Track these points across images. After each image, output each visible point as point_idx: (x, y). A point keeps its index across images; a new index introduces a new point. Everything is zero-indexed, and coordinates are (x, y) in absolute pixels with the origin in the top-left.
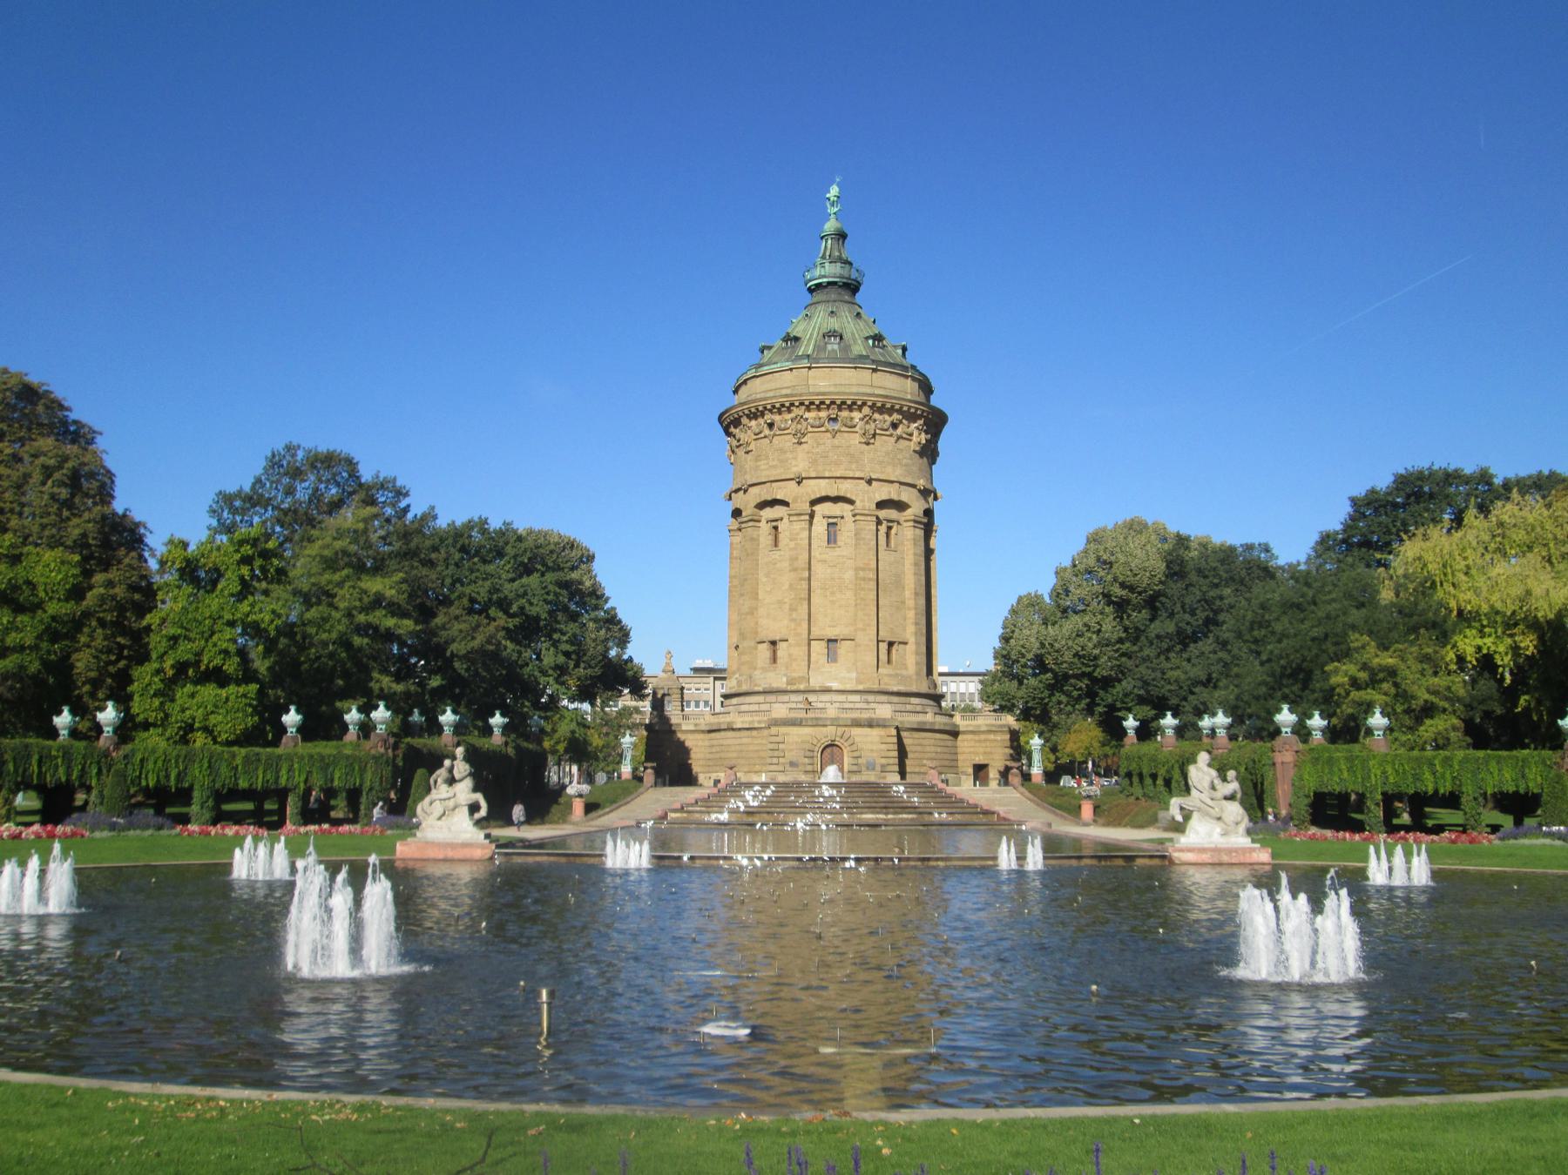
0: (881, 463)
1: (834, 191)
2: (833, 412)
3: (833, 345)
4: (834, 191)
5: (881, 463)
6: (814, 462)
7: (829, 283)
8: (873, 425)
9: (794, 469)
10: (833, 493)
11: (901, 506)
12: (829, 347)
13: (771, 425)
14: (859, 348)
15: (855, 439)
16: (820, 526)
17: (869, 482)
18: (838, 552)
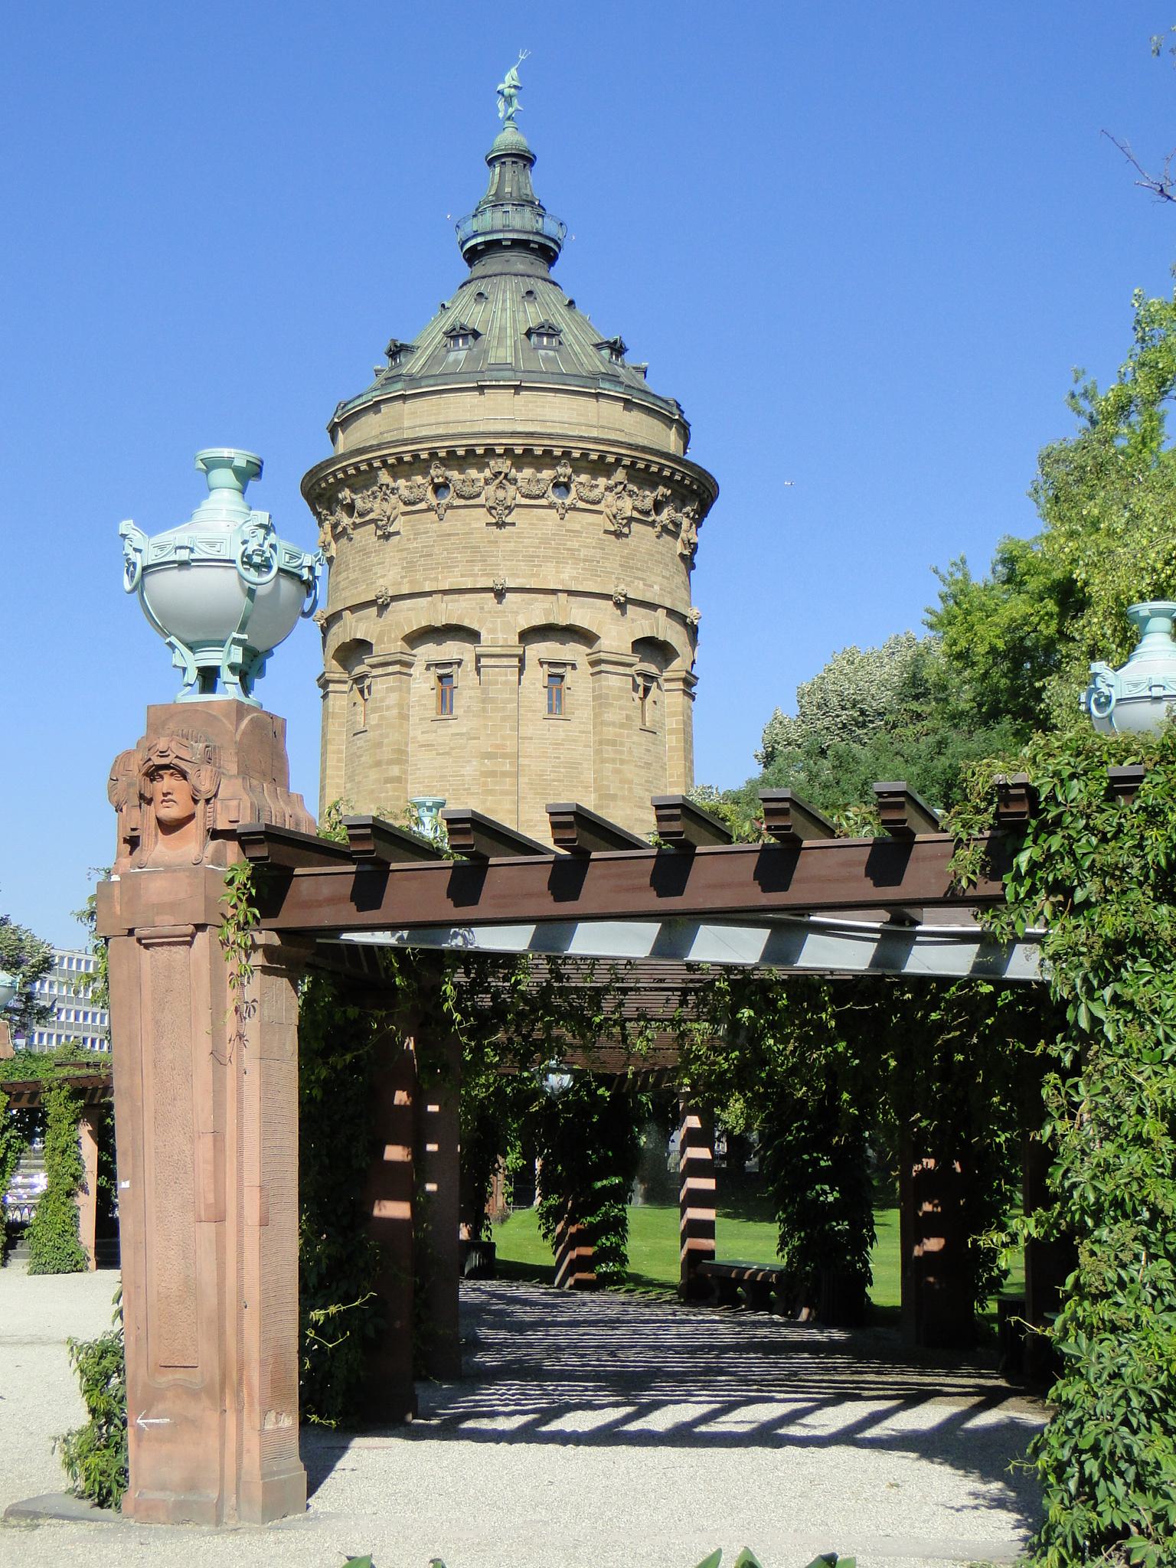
0: (530, 558)
1: (511, 77)
2: (437, 472)
3: (460, 354)
4: (511, 77)
5: (530, 558)
6: (410, 567)
7: (485, 243)
8: (511, 489)
9: (381, 581)
10: (440, 621)
11: (585, 637)
12: (452, 356)
13: (350, 509)
14: (502, 352)
15: (479, 518)
16: (423, 683)
17: (500, 594)
18: (454, 727)
